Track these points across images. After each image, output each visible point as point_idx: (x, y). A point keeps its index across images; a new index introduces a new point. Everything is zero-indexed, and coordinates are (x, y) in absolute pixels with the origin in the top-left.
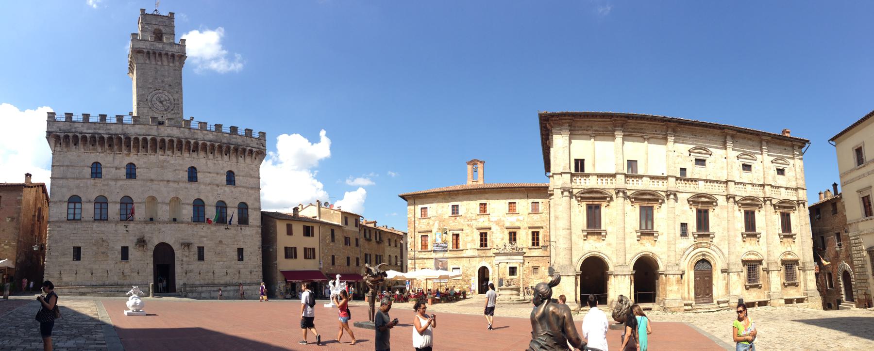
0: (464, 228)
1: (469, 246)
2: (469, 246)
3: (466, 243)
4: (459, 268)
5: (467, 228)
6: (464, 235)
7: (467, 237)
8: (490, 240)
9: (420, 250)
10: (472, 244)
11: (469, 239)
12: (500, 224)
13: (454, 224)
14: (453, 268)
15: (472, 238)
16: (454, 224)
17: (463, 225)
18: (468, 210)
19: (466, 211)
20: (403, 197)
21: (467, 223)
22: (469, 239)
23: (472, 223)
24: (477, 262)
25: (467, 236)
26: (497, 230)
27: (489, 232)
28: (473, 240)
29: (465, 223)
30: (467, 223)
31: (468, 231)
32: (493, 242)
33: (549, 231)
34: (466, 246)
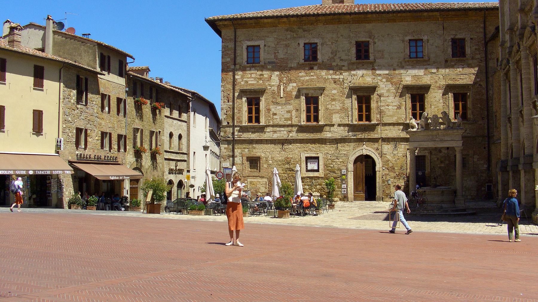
0: (327, 85)
1: (336, 119)
2: (336, 119)
3: (331, 114)
4: (317, 158)
5: (334, 86)
6: (327, 99)
7: (334, 103)
8: (378, 107)
9: (245, 123)
10: (343, 114)
11: (337, 106)
12: (394, 80)
13: (307, 78)
14: (307, 158)
15: (341, 105)
16: (307, 78)
17: (326, 80)
18: (334, 53)
19: (331, 56)
20: (214, 24)
21: (334, 77)
22: (337, 106)
23: (342, 77)
24: (352, 148)
25: (333, 100)
26: (388, 91)
27: (374, 97)
28: (344, 109)
29: (330, 77)
30: (334, 77)
31: (334, 92)
32: (381, 112)
33: (484, 91)
34: (331, 119)
